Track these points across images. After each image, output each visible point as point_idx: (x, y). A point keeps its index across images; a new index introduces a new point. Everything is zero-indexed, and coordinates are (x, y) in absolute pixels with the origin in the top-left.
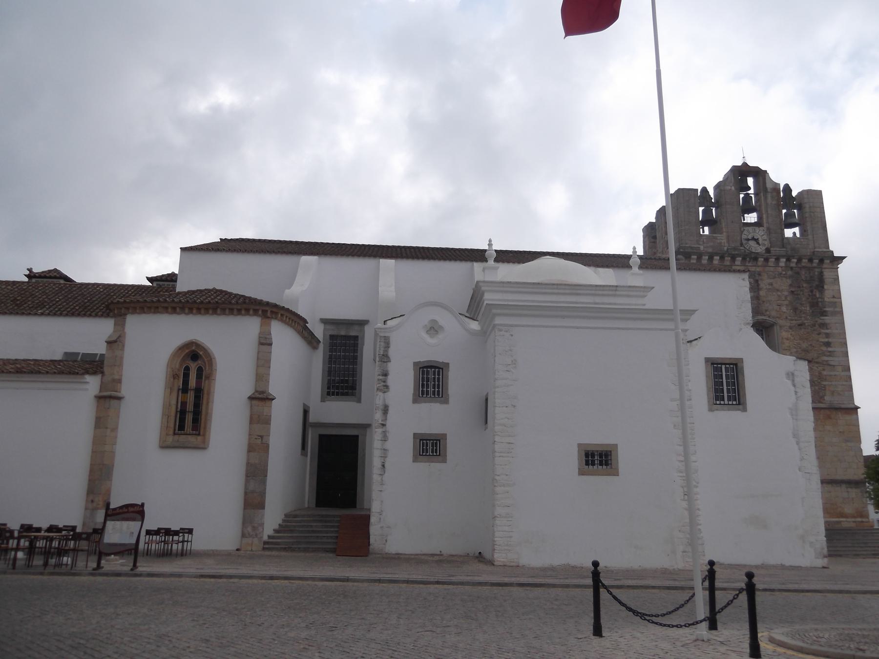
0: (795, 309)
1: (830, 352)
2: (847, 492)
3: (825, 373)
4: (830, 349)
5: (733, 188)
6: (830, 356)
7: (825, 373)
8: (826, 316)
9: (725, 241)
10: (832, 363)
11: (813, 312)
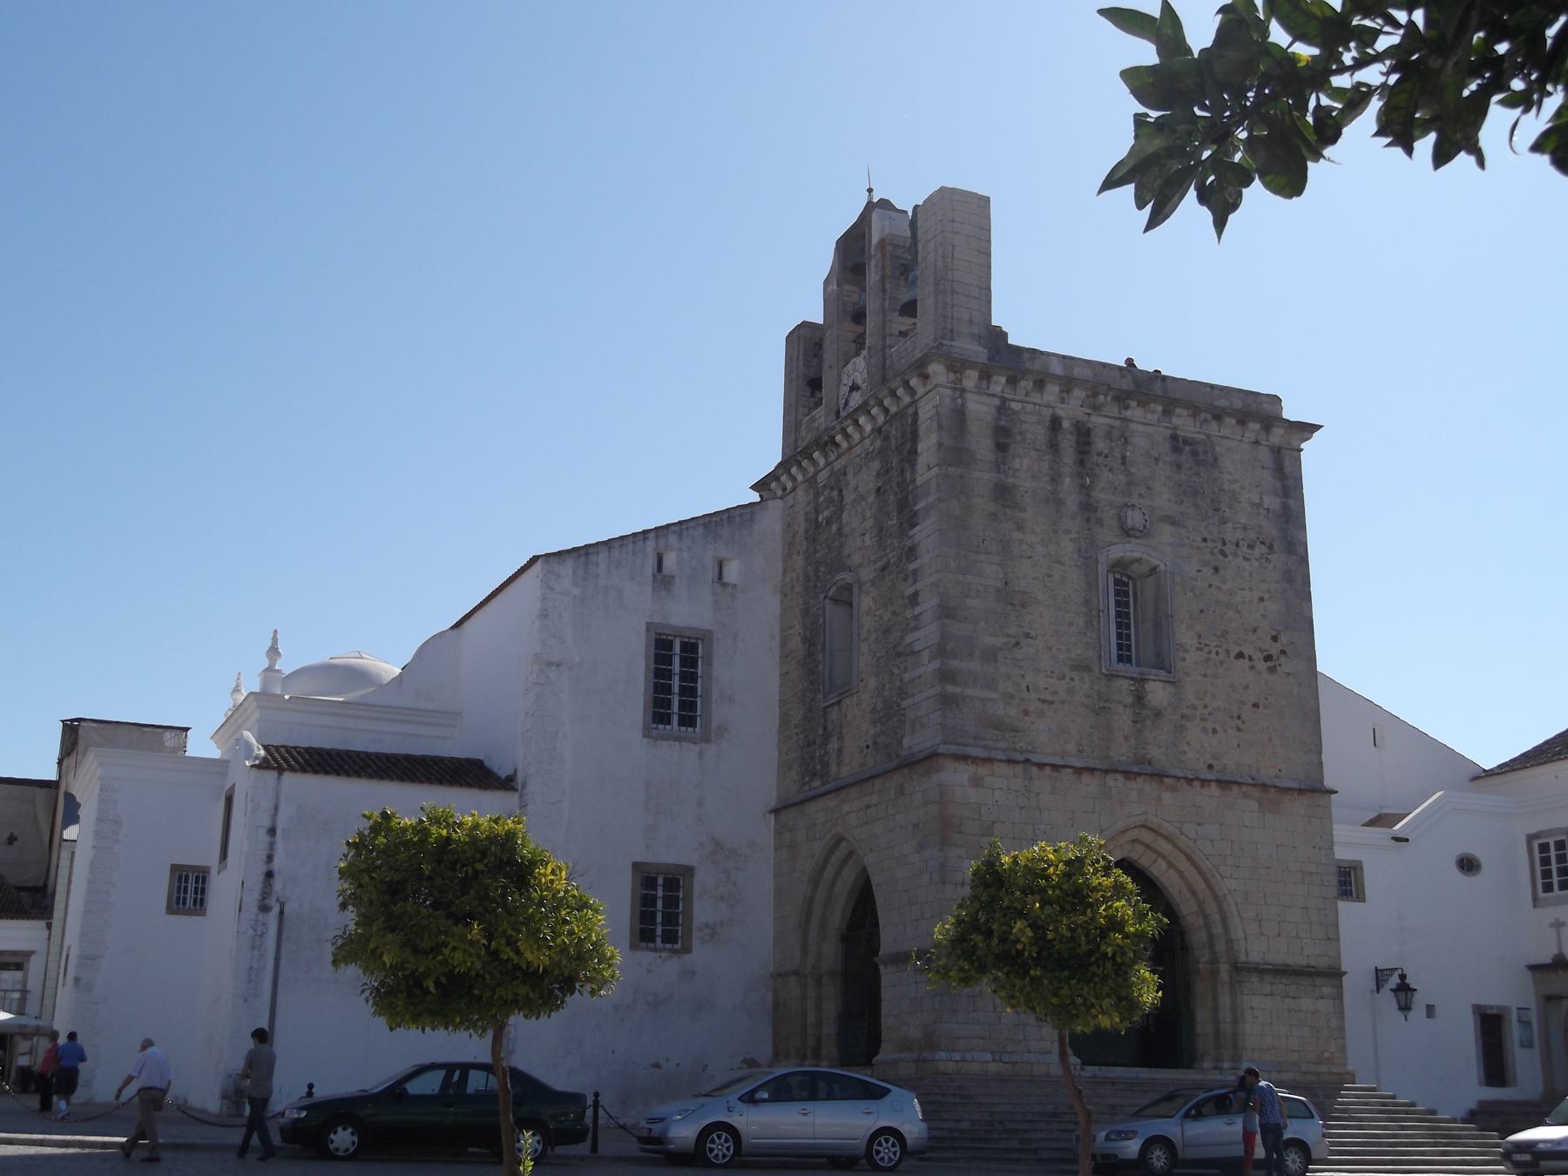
0: (881, 532)
1: (916, 617)
2: (916, 982)
3: (907, 676)
4: (917, 610)
5: (835, 287)
6: (916, 628)
7: (907, 676)
8: (916, 524)
9: (823, 418)
10: (917, 647)
11: (901, 525)
